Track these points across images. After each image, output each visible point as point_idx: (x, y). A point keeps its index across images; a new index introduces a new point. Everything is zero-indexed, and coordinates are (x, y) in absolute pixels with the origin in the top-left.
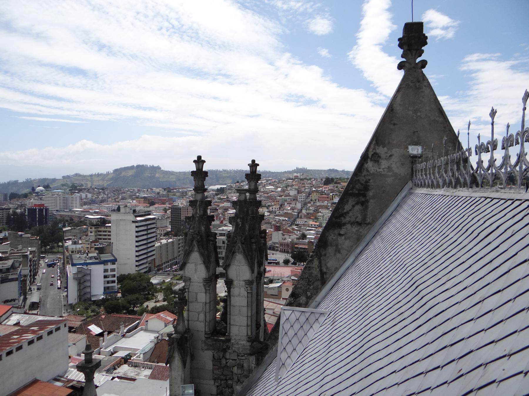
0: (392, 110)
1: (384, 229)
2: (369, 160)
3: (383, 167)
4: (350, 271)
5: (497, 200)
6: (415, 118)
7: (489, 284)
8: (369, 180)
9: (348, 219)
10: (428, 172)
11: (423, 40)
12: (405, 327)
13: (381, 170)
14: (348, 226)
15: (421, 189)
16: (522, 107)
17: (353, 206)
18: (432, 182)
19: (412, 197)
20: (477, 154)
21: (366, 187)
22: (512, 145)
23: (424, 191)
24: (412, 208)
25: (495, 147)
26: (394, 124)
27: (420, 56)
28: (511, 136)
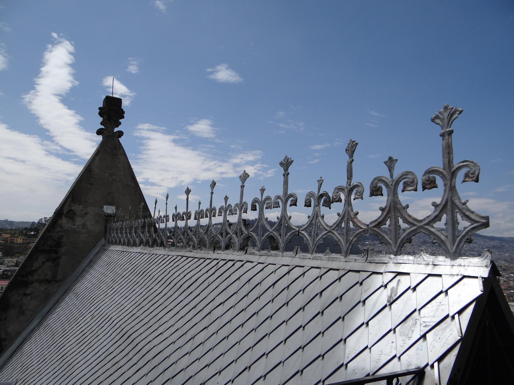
0: (90, 171)
1: (78, 285)
2: (64, 217)
3: (77, 223)
4: (37, 333)
5: (192, 259)
6: (110, 180)
7: (196, 324)
8: (63, 236)
9: (36, 277)
10: (124, 231)
11: (121, 114)
12: (123, 374)
13: (76, 227)
14: (36, 285)
15: (115, 246)
16: (211, 191)
17: (43, 263)
18: (129, 240)
19: (107, 253)
20: (173, 221)
21: (59, 244)
22: (202, 217)
23: (119, 248)
24: (109, 264)
25: (189, 217)
26: (91, 184)
27: (118, 126)
28: (202, 211)
